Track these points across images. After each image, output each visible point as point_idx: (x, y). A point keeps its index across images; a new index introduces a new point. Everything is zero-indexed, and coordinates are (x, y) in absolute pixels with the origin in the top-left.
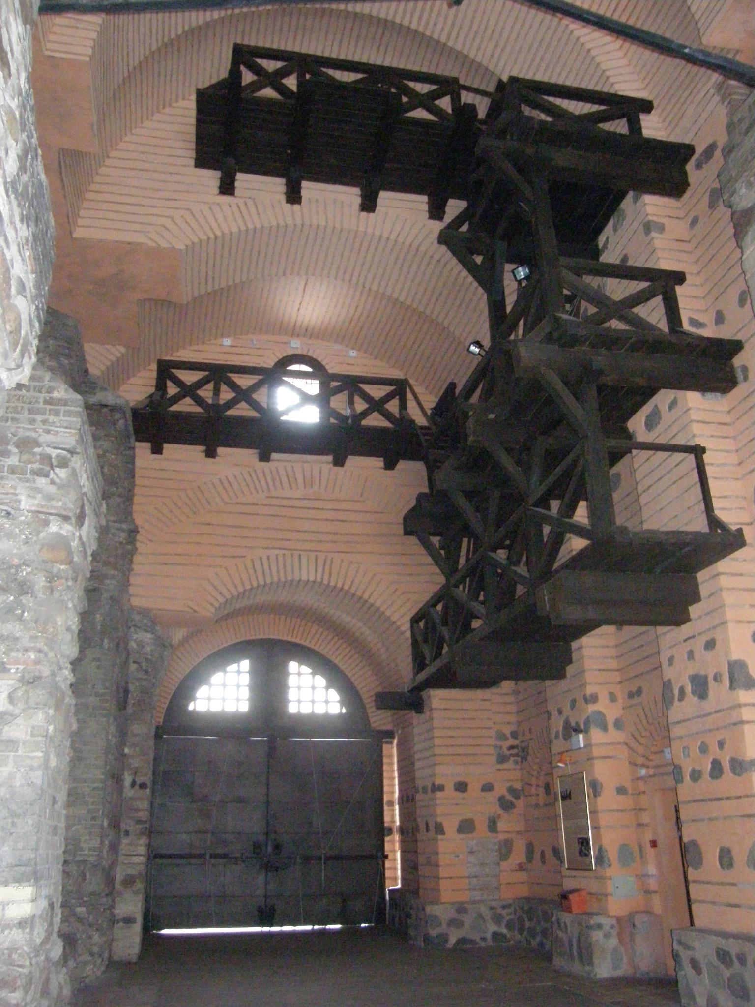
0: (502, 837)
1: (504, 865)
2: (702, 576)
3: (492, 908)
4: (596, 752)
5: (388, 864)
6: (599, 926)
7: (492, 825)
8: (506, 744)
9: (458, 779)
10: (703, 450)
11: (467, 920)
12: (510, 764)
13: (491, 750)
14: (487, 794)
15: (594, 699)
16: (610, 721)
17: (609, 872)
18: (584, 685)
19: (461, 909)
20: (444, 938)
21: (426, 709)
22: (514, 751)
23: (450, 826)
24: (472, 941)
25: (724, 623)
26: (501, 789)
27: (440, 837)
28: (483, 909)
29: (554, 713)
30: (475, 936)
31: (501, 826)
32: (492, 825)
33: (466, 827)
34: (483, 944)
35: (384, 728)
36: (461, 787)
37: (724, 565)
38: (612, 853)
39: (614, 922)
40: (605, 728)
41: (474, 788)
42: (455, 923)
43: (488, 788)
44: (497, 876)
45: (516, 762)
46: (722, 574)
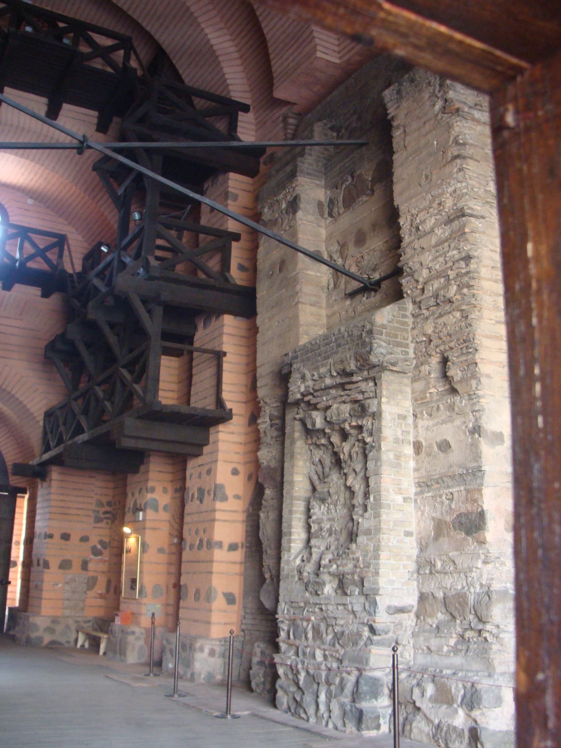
0: (90, 574)
1: (91, 594)
2: (212, 430)
3: (77, 622)
4: (148, 524)
5: (10, 588)
6: (133, 633)
7: (85, 565)
8: (102, 510)
9: (64, 531)
10: (225, 354)
11: (59, 628)
12: (103, 525)
13: (91, 513)
14: (83, 544)
15: (153, 490)
16: (161, 506)
17: (144, 601)
18: (147, 480)
19: (55, 621)
20: (40, 639)
21: (47, 479)
22: (108, 515)
23: (54, 563)
24: (60, 644)
25: (216, 461)
26: (94, 541)
27: (46, 570)
28: (71, 622)
29: (130, 495)
30: (63, 640)
31: (91, 566)
32: (85, 565)
33: (65, 565)
34: (66, 645)
35: (20, 485)
36: (66, 537)
37: (221, 427)
38: (149, 589)
39: (144, 631)
40: (156, 509)
41: (75, 538)
42: (50, 630)
43: (84, 539)
44: (84, 601)
45: (107, 523)
46: (221, 431)
